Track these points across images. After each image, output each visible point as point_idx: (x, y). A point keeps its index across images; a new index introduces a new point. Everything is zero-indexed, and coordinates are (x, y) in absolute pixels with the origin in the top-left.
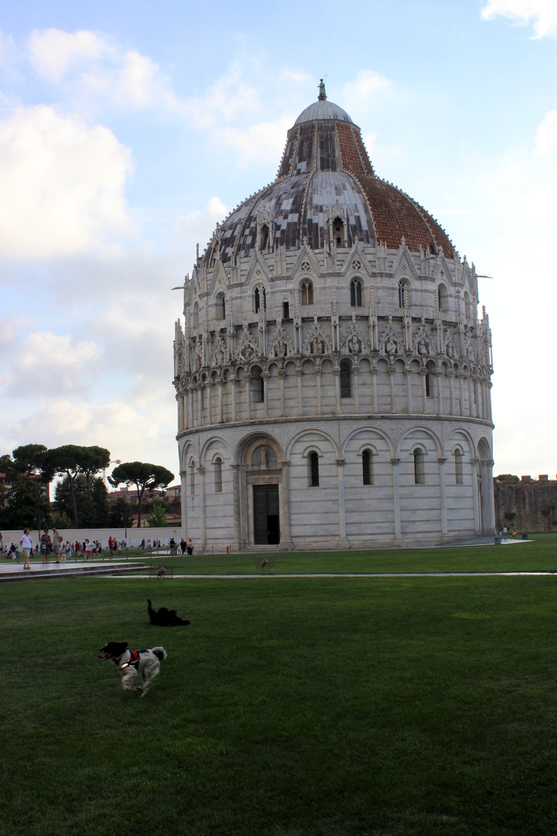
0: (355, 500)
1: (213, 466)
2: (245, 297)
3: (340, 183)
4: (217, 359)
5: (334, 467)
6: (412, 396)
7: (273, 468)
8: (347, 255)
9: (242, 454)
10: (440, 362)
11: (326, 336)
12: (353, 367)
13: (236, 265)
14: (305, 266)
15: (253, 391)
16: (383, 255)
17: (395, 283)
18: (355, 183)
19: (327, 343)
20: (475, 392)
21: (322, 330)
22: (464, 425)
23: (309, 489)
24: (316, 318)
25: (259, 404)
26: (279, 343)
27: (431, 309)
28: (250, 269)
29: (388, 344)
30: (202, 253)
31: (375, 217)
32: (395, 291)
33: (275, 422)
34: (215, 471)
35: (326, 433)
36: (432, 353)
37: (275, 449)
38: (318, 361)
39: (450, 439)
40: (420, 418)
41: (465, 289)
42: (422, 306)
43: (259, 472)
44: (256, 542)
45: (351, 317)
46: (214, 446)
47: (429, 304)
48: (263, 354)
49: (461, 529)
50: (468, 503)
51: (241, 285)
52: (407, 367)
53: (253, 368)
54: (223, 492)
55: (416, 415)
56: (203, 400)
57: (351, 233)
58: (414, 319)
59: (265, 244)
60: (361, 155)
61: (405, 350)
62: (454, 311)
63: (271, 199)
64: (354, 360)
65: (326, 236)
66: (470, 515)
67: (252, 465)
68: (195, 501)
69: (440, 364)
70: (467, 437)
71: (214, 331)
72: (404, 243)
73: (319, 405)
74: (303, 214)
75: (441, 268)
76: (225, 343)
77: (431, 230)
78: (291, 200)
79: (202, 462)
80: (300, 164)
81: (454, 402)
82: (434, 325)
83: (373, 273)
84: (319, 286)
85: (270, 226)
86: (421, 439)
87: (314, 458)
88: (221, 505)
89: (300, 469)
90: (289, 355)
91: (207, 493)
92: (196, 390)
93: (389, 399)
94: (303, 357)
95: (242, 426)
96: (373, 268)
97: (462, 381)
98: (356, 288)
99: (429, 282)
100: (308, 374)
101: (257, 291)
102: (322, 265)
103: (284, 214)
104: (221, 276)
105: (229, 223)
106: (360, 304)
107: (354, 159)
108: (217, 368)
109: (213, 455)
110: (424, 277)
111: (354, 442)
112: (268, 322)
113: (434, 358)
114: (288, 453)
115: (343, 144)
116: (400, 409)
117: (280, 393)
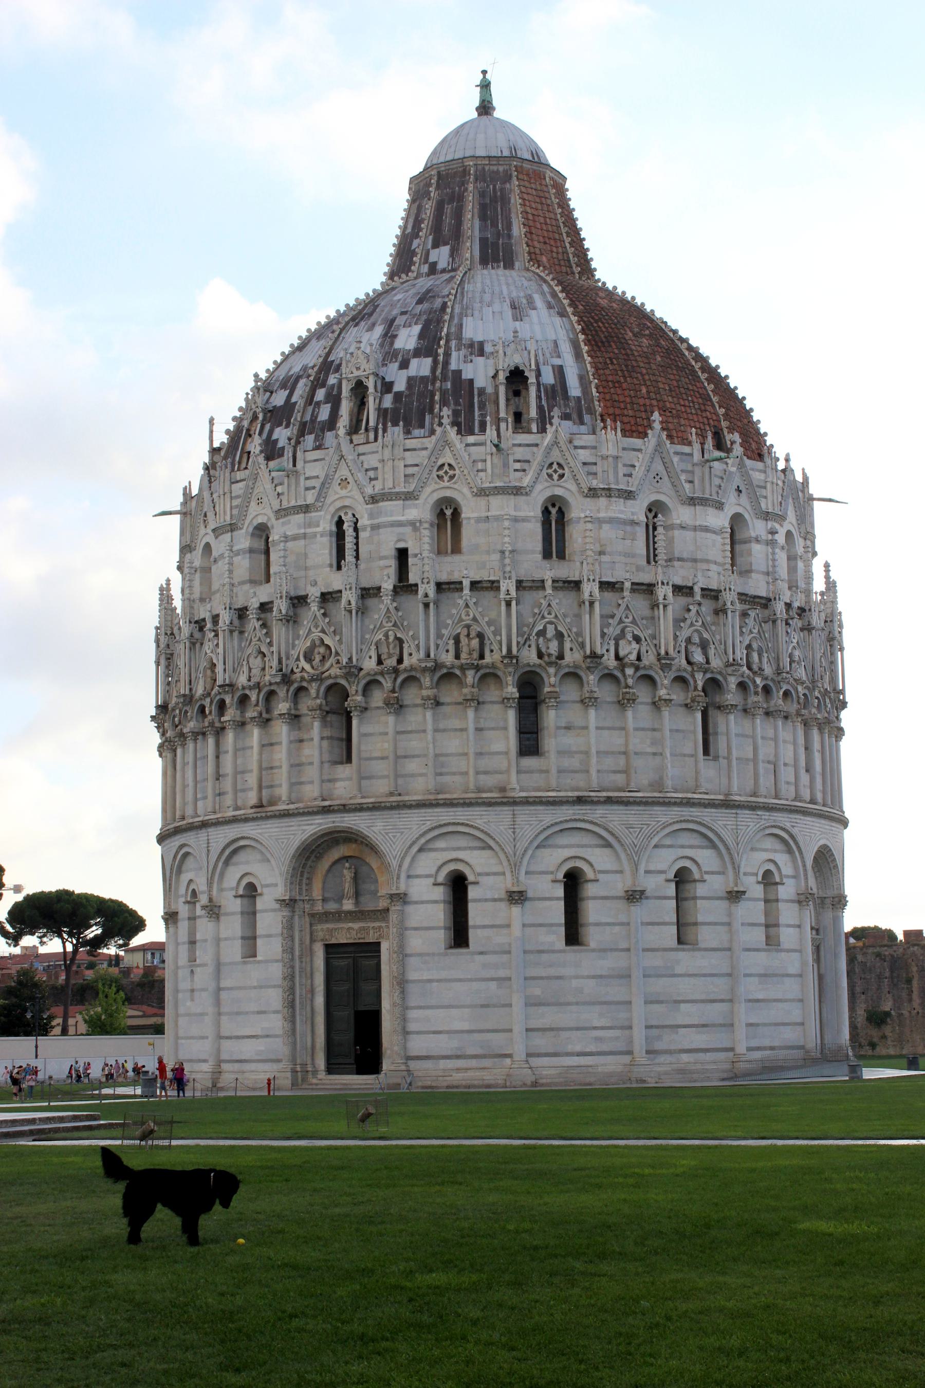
0: (548, 978)
1: (239, 901)
2: (314, 535)
3: (522, 294)
4: (250, 669)
5: (503, 905)
6: (671, 755)
7: (369, 904)
8: (535, 449)
9: (302, 876)
10: (733, 682)
11: (489, 624)
12: (547, 689)
13: (294, 465)
14: (445, 471)
15: (330, 738)
16: (612, 450)
17: (637, 510)
18: (554, 295)
19: (491, 636)
20: (806, 749)
21: (480, 609)
22: (783, 819)
23: (446, 954)
24: (466, 583)
26: (386, 636)
27: (713, 567)
28: (327, 475)
29: (622, 643)
30: (221, 438)
31: (597, 369)
32: (638, 528)
33: (375, 807)
34: (242, 913)
35: (486, 833)
36: (716, 663)
37: (374, 864)
38: (470, 677)
39: (752, 849)
40: (689, 803)
41: (787, 526)
42: (695, 561)
43: (339, 916)
44: (330, 1070)
45: (543, 581)
46: (242, 856)
47: (710, 558)
48: (350, 659)
49: (776, 1044)
50: (791, 988)
51: (306, 509)
52: (662, 692)
53: (329, 688)
54: (259, 958)
55: (680, 795)
56: (217, 757)
57: (544, 403)
58: (679, 590)
59: (359, 421)
60: (568, 234)
61: (659, 654)
62: (763, 573)
63: (374, 325)
64: (549, 676)
65: (490, 407)
66: (796, 1014)
67: (324, 900)
68: (197, 977)
69: (733, 686)
70: (789, 844)
71: (246, 608)
72: (657, 426)
73: (471, 772)
74: (441, 358)
75: (737, 481)
76: (268, 634)
77: (715, 399)
78: (417, 329)
80: (437, 250)
81: (762, 767)
82: (721, 602)
83: (590, 489)
84: (475, 515)
85: (370, 384)
86: (691, 847)
87: (458, 886)
88: (255, 988)
89: (429, 910)
90: (406, 662)
91: (225, 959)
92: (204, 734)
93: (622, 761)
94: (438, 666)
95: (303, 814)
96: (590, 477)
97: (780, 723)
98: (555, 517)
99: (711, 511)
100: (448, 704)
101: (340, 523)
102: (482, 471)
103: (400, 358)
104: (262, 489)
105: (281, 374)
106: (561, 556)
107: (552, 243)
108: (251, 688)
109: (238, 876)
110: (701, 499)
111: (546, 852)
112: (363, 589)
113: (720, 673)
115: (528, 210)
116: (646, 782)
117: (386, 745)
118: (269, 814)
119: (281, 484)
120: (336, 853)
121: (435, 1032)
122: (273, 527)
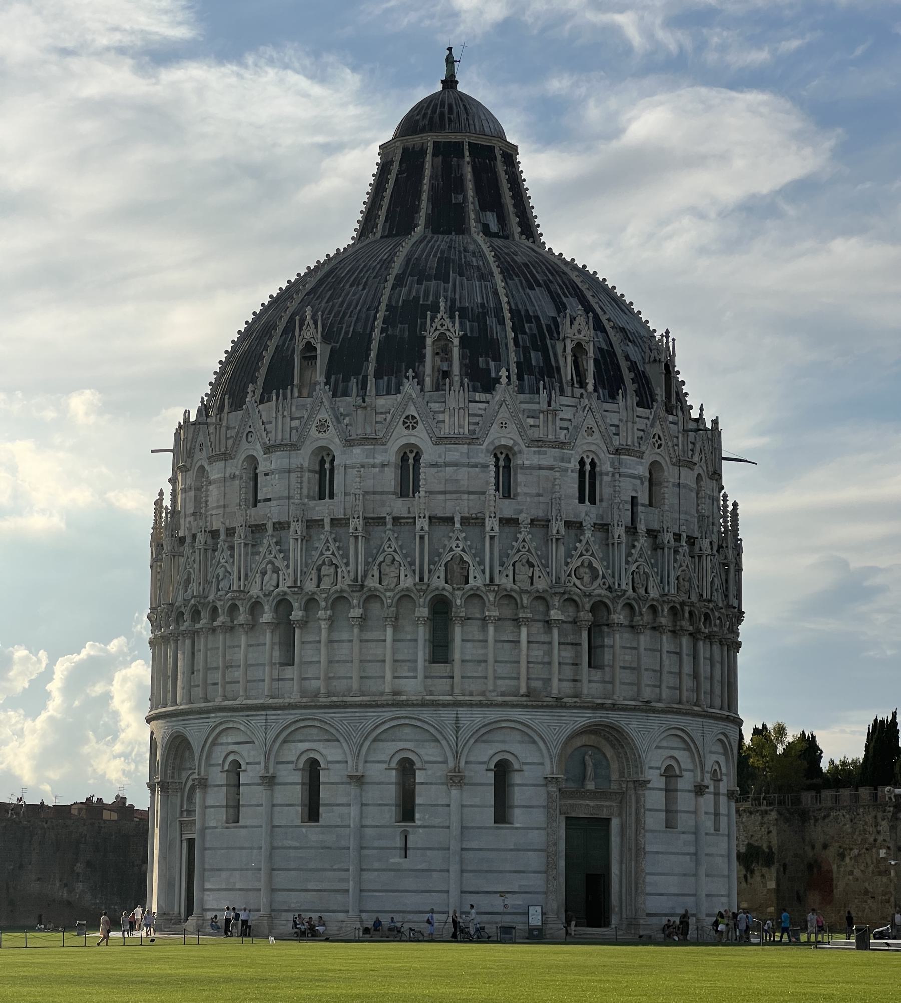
5: (692, 795)
25: (593, 671)
33: (634, 709)
64: (715, 617)
84: (672, 480)
88: (511, 850)
95: (575, 707)
101: (582, 462)
108: (522, 592)
109: (491, 752)
118: (545, 703)
120: (578, 742)
122: (520, 452)
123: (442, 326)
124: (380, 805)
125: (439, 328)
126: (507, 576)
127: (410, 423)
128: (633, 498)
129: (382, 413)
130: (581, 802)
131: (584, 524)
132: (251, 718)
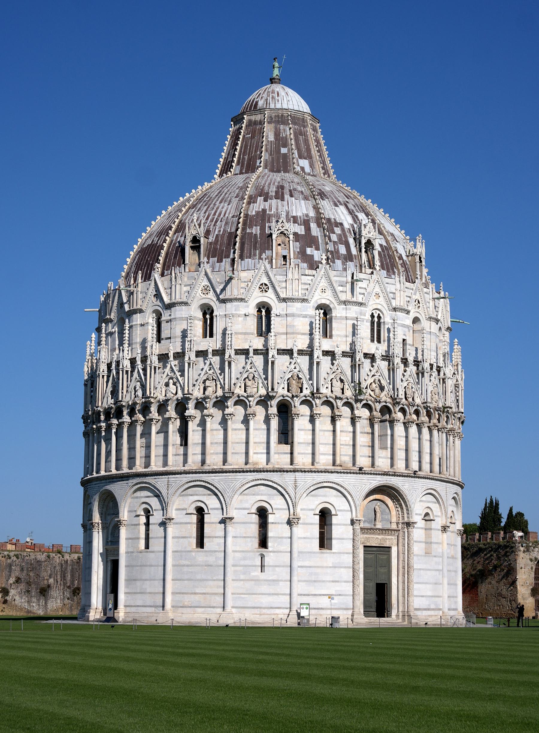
23: (425, 556)
54: (333, 551)
67: (364, 522)
79: (298, 510)
88: (330, 567)
101: (372, 316)
104: (325, 285)
109: (318, 503)
114: (414, 513)
118: (352, 471)
119: (342, 286)
121: (423, 596)
122: (335, 308)
123: (282, 227)
124: (245, 537)
125: (281, 228)
126: (327, 388)
127: (264, 288)
128: (404, 340)
129: (245, 282)
130: (373, 536)
131: (375, 355)
132: (158, 480)
